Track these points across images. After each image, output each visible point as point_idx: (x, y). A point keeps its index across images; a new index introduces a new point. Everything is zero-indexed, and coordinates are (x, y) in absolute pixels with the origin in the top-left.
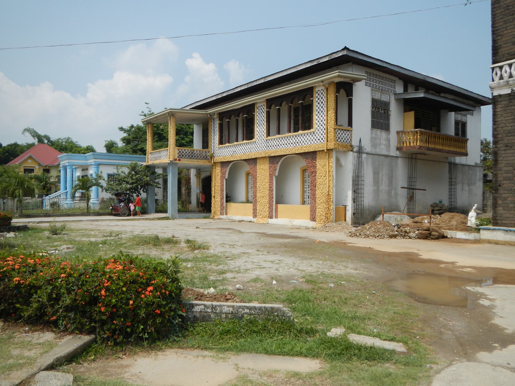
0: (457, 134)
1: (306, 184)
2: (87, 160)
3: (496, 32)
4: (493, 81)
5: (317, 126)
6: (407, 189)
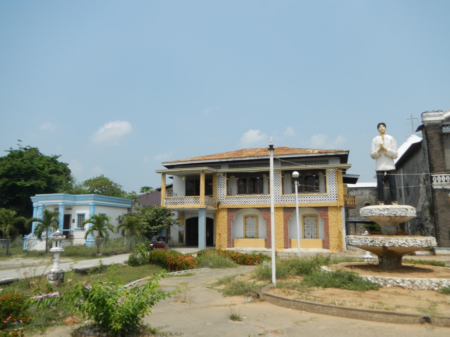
1: (305, 225)
2: (75, 200)
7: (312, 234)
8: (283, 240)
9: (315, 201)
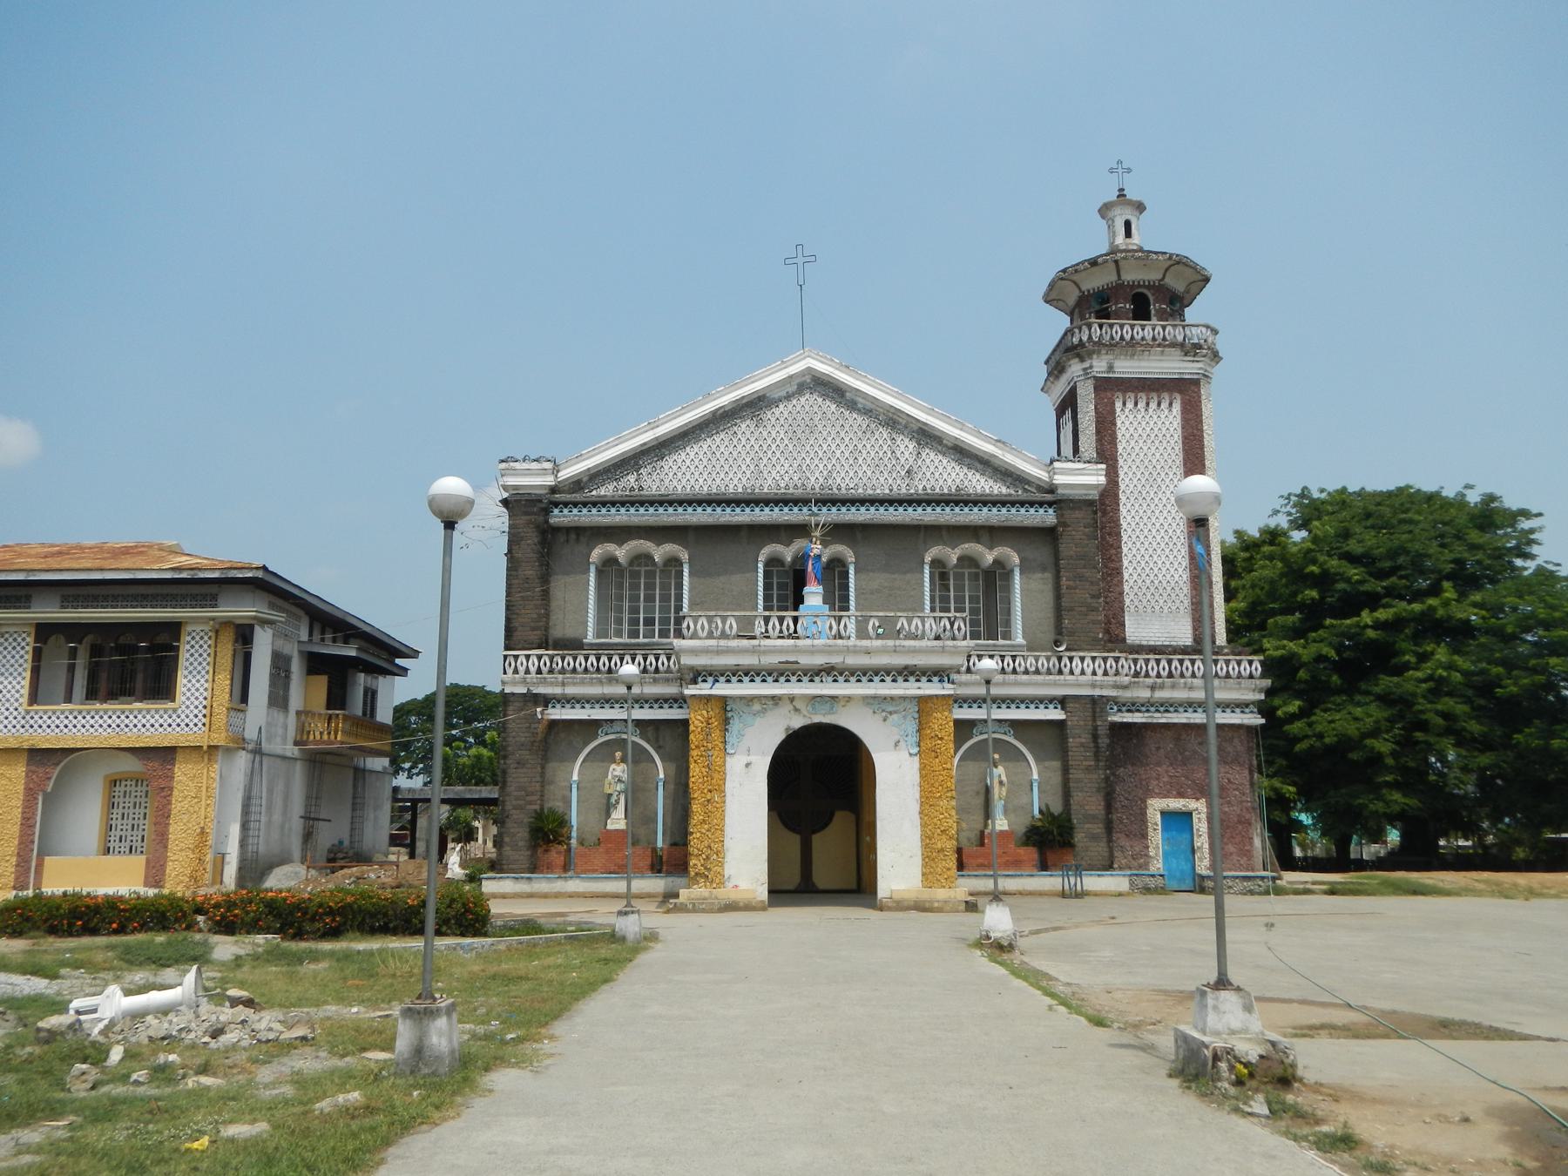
0: (364, 714)
1: (115, 811)
4: (505, 673)
5: (184, 698)
7: (134, 839)
8: (14, 860)
9: (135, 730)
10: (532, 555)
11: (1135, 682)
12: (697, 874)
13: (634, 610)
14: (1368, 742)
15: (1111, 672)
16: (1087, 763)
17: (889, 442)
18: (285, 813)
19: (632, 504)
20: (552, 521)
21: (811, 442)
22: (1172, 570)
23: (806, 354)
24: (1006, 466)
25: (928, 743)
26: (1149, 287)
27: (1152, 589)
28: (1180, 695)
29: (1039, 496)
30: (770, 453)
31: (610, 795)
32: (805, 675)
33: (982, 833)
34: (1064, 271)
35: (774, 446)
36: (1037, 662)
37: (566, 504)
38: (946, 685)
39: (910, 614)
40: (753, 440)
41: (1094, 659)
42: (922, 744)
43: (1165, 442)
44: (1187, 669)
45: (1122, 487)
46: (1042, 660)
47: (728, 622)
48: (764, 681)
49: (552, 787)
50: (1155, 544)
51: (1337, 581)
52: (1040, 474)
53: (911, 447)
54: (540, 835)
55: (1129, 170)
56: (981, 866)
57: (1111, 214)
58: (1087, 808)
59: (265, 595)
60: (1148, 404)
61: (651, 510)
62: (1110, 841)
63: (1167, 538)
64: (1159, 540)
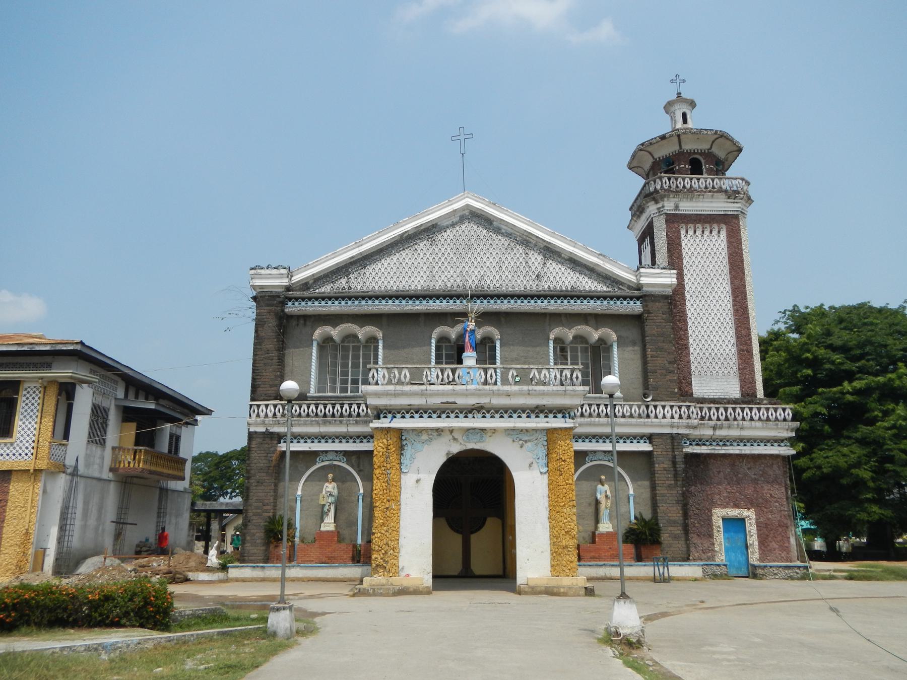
0: (170, 452)
3: (256, 371)
6: (115, 524)
10: (271, 334)
11: (701, 424)
12: (377, 566)
13: (344, 373)
14: (853, 471)
15: (685, 416)
16: (667, 482)
17: (524, 256)
18: (99, 518)
19: (343, 298)
20: (286, 310)
21: (469, 256)
22: (724, 346)
23: (466, 195)
24: (607, 273)
25: (554, 464)
26: (701, 154)
27: (710, 359)
28: (735, 433)
29: (628, 292)
30: (440, 263)
31: (324, 506)
32: (461, 413)
33: (594, 533)
34: (642, 144)
35: (443, 259)
36: (631, 409)
37: (297, 299)
38: (568, 420)
39: (540, 367)
40: (428, 254)
41: (672, 407)
42: (550, 465)
43: (716, 258)
44: (739, 414)
45: (687, 288)
46: (635, 408)
47: (403, 373)
48: (430, 417)
49: (282, 500)
50: (711, 327)
51: (824, 363)
52: (630, 277)
53: (539, 259)
54: (272, 535)
55: (684, 81)
56: (593, 558)
57: (672, 109)
58: (670, 515)
59: (87, 363)
60: (703, 232)
61: (357, 302)
62: (687, 539)
63: (719, 324)
64: (714, 325)
